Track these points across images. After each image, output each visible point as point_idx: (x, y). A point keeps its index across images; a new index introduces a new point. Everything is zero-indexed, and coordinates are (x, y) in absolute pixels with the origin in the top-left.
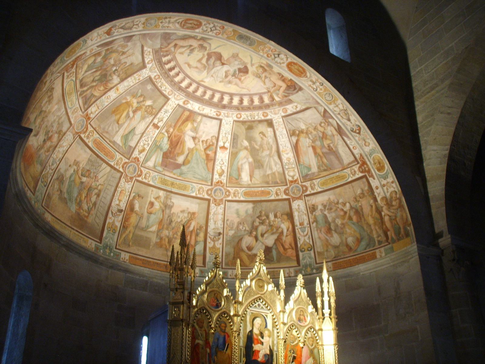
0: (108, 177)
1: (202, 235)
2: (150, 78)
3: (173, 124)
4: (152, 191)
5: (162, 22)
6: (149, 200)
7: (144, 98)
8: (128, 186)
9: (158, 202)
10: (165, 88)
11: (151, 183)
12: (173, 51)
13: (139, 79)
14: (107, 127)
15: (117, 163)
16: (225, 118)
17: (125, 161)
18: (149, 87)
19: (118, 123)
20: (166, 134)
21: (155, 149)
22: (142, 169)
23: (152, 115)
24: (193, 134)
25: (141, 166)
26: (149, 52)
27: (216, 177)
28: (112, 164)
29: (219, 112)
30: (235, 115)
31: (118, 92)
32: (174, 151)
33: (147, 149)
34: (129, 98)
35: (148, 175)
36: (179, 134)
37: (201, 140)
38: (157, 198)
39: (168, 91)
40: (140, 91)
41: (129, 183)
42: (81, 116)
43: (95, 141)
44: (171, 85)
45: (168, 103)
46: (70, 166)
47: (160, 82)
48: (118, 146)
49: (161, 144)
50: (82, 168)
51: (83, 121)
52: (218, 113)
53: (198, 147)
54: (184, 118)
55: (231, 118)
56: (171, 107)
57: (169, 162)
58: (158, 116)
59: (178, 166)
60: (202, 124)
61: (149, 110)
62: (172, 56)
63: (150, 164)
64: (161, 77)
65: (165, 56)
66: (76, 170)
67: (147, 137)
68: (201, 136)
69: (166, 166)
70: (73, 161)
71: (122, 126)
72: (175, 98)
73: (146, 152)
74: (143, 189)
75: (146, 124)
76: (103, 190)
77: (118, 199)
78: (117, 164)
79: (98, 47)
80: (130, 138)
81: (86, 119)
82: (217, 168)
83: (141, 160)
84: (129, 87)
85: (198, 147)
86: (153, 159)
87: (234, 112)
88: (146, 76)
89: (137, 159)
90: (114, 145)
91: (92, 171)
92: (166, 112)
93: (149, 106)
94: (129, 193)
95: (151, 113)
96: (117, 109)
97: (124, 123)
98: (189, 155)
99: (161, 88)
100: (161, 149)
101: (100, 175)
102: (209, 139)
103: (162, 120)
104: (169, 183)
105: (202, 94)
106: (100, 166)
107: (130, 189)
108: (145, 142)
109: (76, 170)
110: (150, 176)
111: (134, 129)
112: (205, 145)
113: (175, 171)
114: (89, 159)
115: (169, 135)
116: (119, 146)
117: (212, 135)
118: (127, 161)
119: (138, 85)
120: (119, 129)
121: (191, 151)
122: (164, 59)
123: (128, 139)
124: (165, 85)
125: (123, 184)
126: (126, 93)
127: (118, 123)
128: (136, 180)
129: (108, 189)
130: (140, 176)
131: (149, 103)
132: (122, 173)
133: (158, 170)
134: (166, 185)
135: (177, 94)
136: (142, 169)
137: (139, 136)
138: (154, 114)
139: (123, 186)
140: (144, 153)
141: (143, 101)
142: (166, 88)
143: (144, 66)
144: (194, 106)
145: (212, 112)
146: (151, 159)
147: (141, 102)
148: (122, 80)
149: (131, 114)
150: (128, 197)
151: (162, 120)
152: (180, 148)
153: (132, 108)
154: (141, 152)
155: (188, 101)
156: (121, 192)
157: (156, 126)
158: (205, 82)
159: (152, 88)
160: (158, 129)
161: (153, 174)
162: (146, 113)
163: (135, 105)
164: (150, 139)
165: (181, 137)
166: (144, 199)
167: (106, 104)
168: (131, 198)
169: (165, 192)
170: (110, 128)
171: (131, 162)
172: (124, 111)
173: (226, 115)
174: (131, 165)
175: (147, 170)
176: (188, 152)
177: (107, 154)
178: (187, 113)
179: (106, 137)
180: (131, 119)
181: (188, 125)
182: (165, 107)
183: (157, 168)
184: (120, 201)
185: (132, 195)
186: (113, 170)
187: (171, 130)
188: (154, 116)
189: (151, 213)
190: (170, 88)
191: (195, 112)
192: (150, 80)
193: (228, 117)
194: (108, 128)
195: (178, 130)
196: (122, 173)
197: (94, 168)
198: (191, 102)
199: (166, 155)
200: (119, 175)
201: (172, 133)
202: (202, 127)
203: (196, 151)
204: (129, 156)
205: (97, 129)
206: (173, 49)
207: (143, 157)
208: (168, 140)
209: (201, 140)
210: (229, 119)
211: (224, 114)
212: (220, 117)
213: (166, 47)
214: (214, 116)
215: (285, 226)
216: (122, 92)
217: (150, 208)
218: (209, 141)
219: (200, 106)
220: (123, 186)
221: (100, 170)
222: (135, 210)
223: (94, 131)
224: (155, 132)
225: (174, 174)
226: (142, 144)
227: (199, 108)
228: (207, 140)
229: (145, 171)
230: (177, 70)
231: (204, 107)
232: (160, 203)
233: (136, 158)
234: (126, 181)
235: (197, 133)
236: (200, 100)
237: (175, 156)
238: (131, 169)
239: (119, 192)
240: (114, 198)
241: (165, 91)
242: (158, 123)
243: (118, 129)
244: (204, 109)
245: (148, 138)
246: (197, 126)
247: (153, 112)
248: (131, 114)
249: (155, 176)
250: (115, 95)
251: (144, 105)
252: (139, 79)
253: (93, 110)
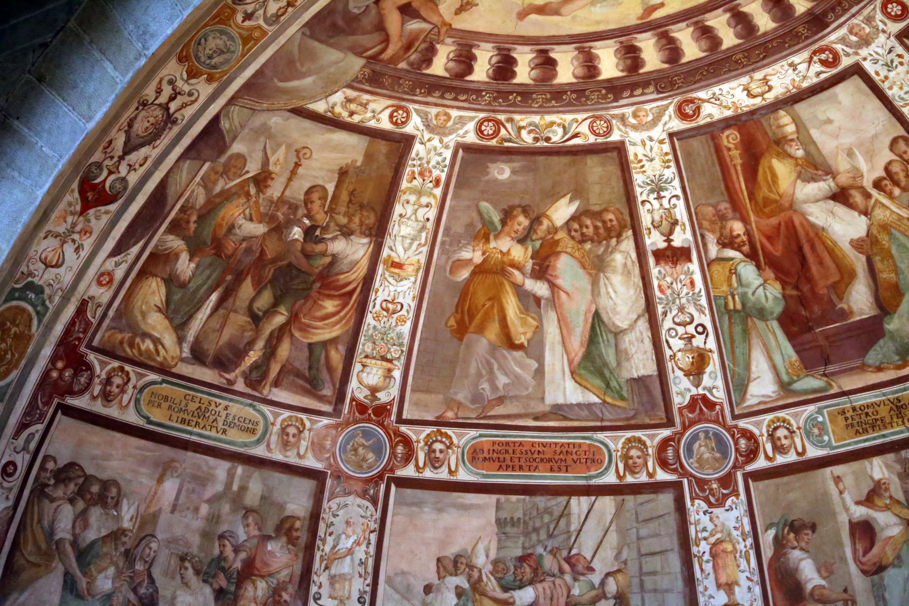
0: (622, 533)
2: (468, 148)
3: (724, 206)
4: (838, 480)
5: (248, 16)
6: (843, 519)
7: (525, 211)
8: (732, 516)
9: (887, 508)
10: (560, 131)
11: (813, 452)
12: (427, 26)
13: (437, 182)
14: (486, 386)
15: (626, 466)
16: (864, 52)
17: (657, 440)
18: (502, 172)
19: (512, 345)
20: (730, 253)
21: (738, 329)
22: (743, 424)
23: (619, 236)
24: (824, 186)
25: (735, 417)
26: (349, 100)
28: (610, 478)
29: (821, 50)
30: (879, 16)
31: (410, 269)
32: (812, 290)
33: (712, 344)
34: (473, 254)
35: (781, 433)
36: (774, 221)
37: (867, 183)
38: (873, 496)
39: (584, 128)
40: (485, 205)
41: (729, 502)
42: (336, 427)
43: (475, 456)
44: (569, 104)
45: (631, 157)
46: (428, 589)
47: (520, 128)
48: (585, 413)
49: (744, 296)
50: (490, 567)
51: (367, 434)
52: (823, 56)
53: (879, 214)
54: (738, 161)
55: (882, 38)
56: (657, 163)
57: (827, 338)
58: (646, 220)
59: (871, 331)
60: (815, 133)
61: (590, 231)
62: (449, 40)
63: (762, 387)
64: (502, 117)
65: (428, 62)
66: (466, 585)
67: (675, 312)
68: (857, 173)
69: (827, 362)
70: (433, 566)
71: (541, 345)
72: (635, 128)
73: (715, 356)
74: (796, 494)
75: (627, 273)
76: (636, 588)
77: (719, 586)
78: (631, 469)
79: (118, 250)
80: (611, 358)
81: (369, 420)
83: (719, 395)
84: (430, 225)
85: (879, 214)
86: (760, 365)
87: (866, 12)
88: (448, 154)
89: (701, 405)
90: (566, 418)
91: (540, 550)
92: (658, 188)
93: (573, 218)
94: (750, 541)
95: (608, 230)
96: (464, 310)
97: (539, 330)
98: (879, 266)
99: (548, 139)
100: (762, 314)
101: (586, 547)
102: (890, 163)
103: (676, 223)
104: (884, 412)
105: (704, 44)
106: (565, 513)
107: (746, 521)
108: (681, 330)
109: (466, 585)
110: (792, 432)
111: (597, 322)
112: (897, 191)
113: (872, 357)
114: (500, 523)
115: (746, 248)
116: (589, 406)
117: (887, 141)
118: (666, 433)
119: (455, 196)
120: (540, 360)
121: (868, 245)
122: (439, 67)
123: (606, 364)
124: (552, 124)
125: (705, 520)
126: (443, 251)
127: (512, 345)
128: (746, 476)
129: (654, 573)
130: (752, 454)
131: (562, 211)
132: (676, 486)
133: (806, 392)
134: (873, 427)
135: (628, 111)
136: (743, 424)
137: (643, 325)
138: (623, 227)
139: (710, 527)
140: (714, 366)
141: (536, 221)
142: (573, 126)
143: (401, 145)
144: (728, 97)
145: (802, 67)
146: (753, 368)
147: (531, 230)
148: (378, 232)
149: (541, 289)
150: (752, 553)
151: (676, 223)
152: (821, 263)
153: (519, 268)
154: (696, 370)
155: (692, 101)
156: (714, 556)
157: (673, 255)
158: (662, 5)
159: (516, 165)
160: (690, 260)
161: (796, 416)
162: (588, 246)
163: (518, 253)
164: (692, 309)
165: (791, 226)
166: (820, 529)
167: (406, 329)
168: (768, 552)
169: (891, 457)
170: (502, 380)
171: (685, 428)
172: (496, 299)
173: (854, 38)
174: (695, 438)
175: (769, 417)
176: (863, 258)
177: (560, 460)
178: (730, 138)
179: (508, 417)
180: (554, 302)
181: (771, 169)
182: (638, 178)
183: (797, 386)
184: (729, 587)
185: (767, 538)
186: (630, 501)
187: (738, 227)
188: (630, 232)
189: (880, 568)
190: (580, 116)
191: (752, 113)
192: (474, 157)
193: (866, 41)
194: (494, 387)
195: (759, 211)
196: (676, 486)
197: (543, 535)
198: (702, 94)
199: (794, 323)
200: (666, 499)
201: (748, 233)
202: (827, 144)
203: (890, 234)
204: (662, 414)
205: (450, 415)
206: (414, 25)
207: (720, 383)
208: (758, 267)
209: (867, 183)
211: (843, 40)
212: (846, 62)
213: (387, 40)
214: (823, 76)
216: (423, 259)
217: (865, 553)
218: (896, 168)
219: (744, 80)
220: (710, 527)
221: (574, 527)
222: (809, 587)
223: (444, 430)
224: (689, 273)
225: (879, 369)
226: (677, 344)
227: (746, 89)
228: (886, 169)
229: (759, 426)
230: (524, 58)
231: (758, 75)
232: (897, 509)
233: (694, 400)
234: (710, 505)
235: (830, 172)
236: (718, 66)
237: (831, 301)
238: (702, 449)
239: (707, 557)
240: (700, 589)
241: (576, 135)
242: (669, 241)
243: (535, 365)
244: (765, 80)
245: (681, 309)
246: (807, 153)
247: (613, 221)
248: (541, 289)
249: (811, 419)
250: (406, 285)
251: (554, 230)
252: (437, 182)
253: (366, 378)
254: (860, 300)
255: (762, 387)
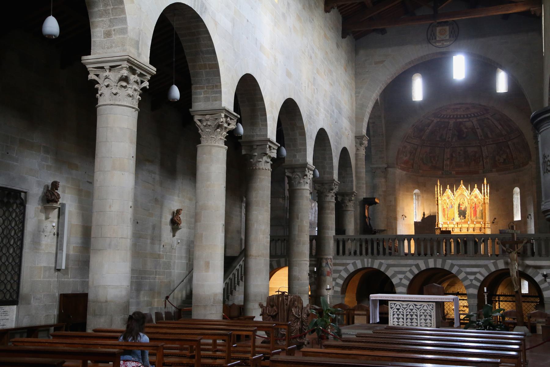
1: (481, 158)
27: (480, 138)
63: (454, 140)
82: (479, 135)
144: (461, 120)
154: (449, 138)
157: (450, 130)
210: (474, 120)
215: (508, 151)
236: (460, 118)
254: (464, 135)
255: (454, 140)
